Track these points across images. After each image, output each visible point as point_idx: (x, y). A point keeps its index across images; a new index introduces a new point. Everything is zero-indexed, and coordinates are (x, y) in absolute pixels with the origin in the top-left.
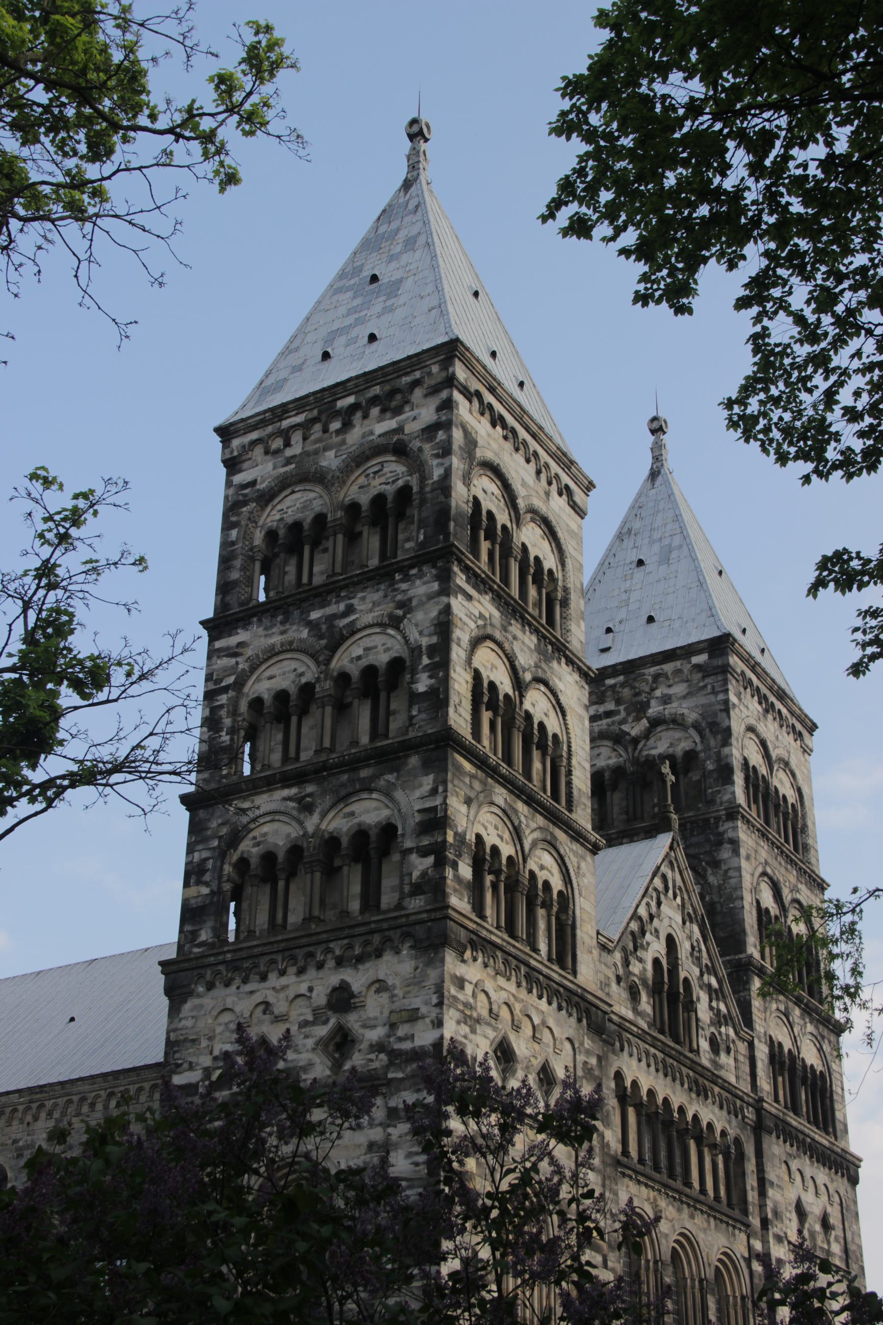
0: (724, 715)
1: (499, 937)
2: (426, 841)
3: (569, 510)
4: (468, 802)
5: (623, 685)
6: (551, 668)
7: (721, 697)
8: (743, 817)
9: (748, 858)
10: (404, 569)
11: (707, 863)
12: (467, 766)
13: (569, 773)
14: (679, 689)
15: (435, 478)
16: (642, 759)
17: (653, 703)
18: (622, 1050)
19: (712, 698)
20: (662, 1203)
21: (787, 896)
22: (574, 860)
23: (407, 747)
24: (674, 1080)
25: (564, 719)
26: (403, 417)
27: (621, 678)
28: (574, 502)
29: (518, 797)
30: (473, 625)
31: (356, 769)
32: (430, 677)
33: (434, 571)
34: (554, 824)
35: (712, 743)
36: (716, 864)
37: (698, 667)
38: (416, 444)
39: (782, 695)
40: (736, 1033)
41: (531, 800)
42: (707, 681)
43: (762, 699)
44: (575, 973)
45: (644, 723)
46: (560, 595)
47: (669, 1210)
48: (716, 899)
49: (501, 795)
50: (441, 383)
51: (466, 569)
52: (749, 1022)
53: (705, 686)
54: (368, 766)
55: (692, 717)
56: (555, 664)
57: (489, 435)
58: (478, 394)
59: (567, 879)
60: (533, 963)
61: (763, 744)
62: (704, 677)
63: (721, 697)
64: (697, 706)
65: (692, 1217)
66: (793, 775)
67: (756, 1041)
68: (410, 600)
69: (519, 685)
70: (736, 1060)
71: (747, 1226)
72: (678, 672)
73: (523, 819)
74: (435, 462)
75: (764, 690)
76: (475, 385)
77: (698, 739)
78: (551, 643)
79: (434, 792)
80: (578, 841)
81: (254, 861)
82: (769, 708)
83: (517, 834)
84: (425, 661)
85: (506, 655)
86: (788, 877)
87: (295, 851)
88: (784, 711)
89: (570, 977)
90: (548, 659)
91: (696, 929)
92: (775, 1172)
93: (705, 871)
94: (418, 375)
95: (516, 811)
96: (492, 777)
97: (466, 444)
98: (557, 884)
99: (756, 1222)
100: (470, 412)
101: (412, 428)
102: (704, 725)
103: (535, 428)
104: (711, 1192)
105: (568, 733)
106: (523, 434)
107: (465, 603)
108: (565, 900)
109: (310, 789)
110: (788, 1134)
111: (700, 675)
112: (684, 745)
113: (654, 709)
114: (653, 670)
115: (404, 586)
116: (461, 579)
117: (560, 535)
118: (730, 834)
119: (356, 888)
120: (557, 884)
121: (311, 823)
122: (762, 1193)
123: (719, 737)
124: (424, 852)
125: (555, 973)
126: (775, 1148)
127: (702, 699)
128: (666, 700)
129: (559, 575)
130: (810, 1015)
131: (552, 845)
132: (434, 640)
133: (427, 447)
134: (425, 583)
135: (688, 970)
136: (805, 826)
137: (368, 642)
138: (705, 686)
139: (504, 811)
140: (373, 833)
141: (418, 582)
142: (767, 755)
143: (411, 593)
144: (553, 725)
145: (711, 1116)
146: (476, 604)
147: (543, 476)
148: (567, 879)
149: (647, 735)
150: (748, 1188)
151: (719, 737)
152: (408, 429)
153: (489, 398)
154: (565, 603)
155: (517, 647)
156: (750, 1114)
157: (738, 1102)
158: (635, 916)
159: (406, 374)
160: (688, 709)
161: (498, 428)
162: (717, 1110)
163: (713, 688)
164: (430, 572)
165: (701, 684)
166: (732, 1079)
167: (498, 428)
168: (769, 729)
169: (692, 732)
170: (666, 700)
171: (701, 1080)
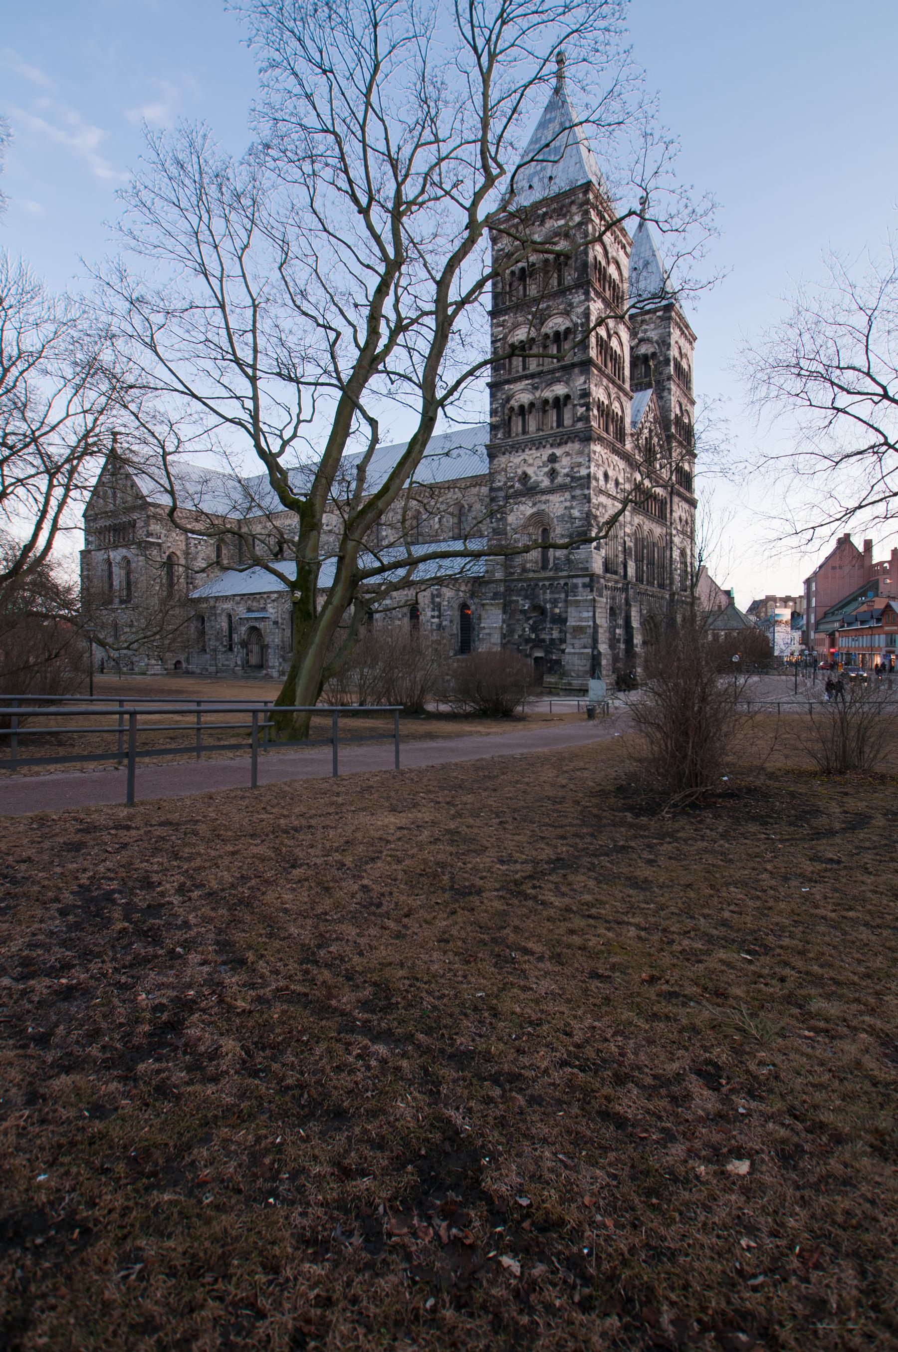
1: (605, 435)
2: (582, 401)
23: (573, 365)
37: (659, 317)
39: (687, 327)
41: (613, 382)
43: (681, 329)
47: (647, 522)
49: (605, 382)
55: (655, 338)
79: (585, 382)
81: (516, 408)
82: (683, 333)
83: (609, 396)
86: (684, 401)
87: (532, 405)
98: (620, 413)
109: (537, 380)
112: (652, 350)
113: (640, 335)
119: (555, 418)
120: (620, 413)
121: (537, 394)
124: (582, 406)
125: (619, 445)
127: (660, 331)
128: (645, 331)
131: (619, 398)
142: (680, 353)
144: (619, 352)
148: (623, 411)
160: (654, 335)
168: (682, 341)
170: (645, 331)
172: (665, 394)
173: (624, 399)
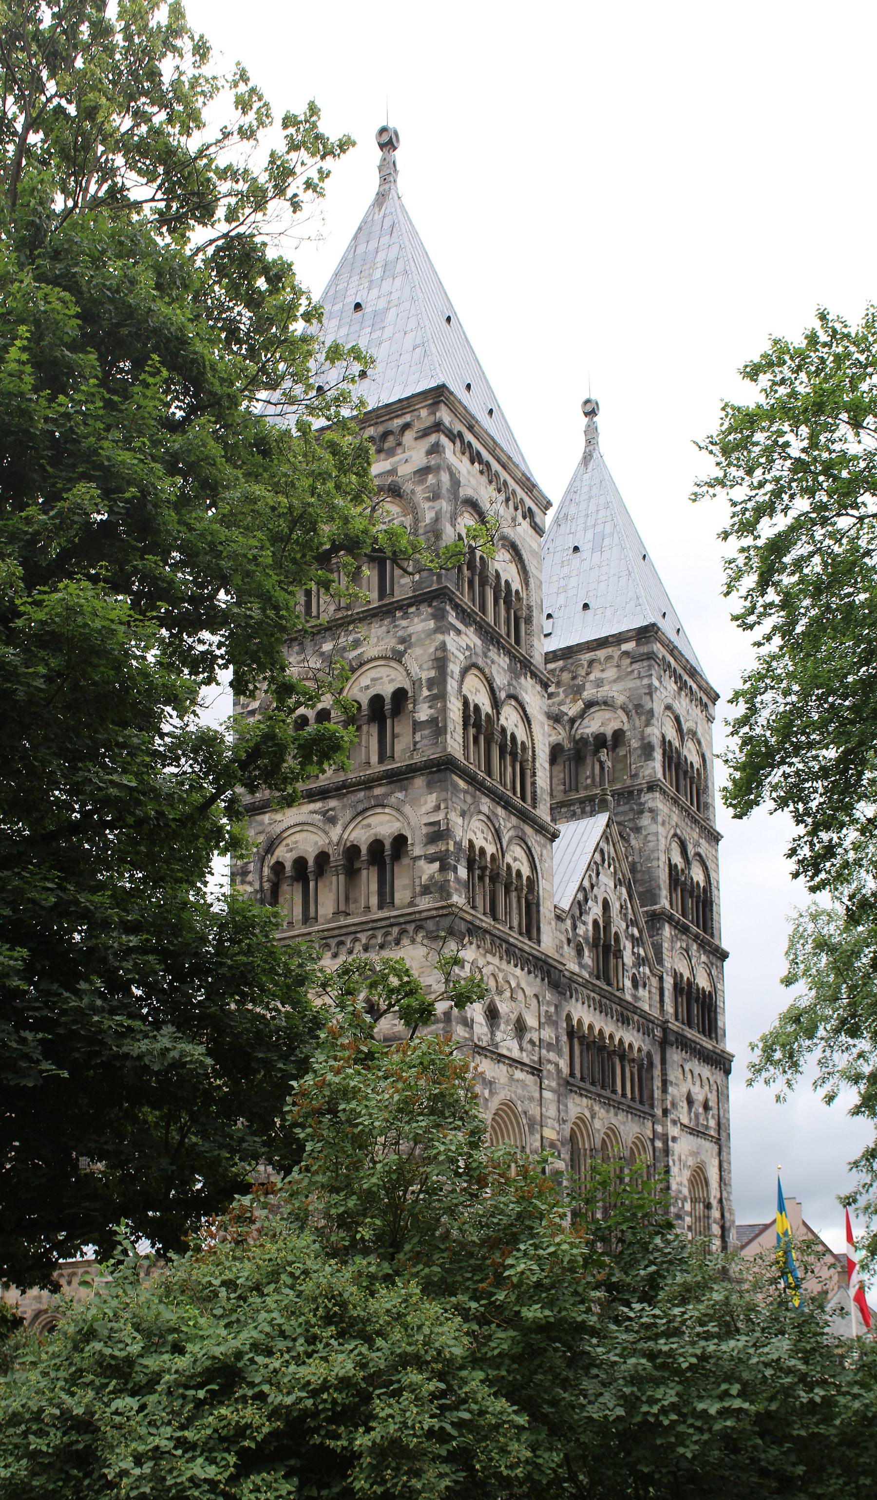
0: (648, 697)
1: (487, 922)
2: (432, 850)
3: (531, 531)
4: (463, 814)
5: (562, 670)
6: (520, 684)
7: (645, 681)
8: (661, 789)
9: (663, 824)
10: (403, 607)
11: (631, 829)
12: (462, 784)
13: (534, 774)
14: (611, 673)
15: (428, 521)
16: (578, 737)
17: (587, 685)
18: (571, 997)
19: (638, 682)
20: (596, 1108)
21: (691, 851)
22: (538, 849)
23: (412, 770)
24: (606, 1015)
25: (530, 728)
26: (396, 459)
27: (560, 663)
28: (535, 523)
29: (498, 803)
30: (462, 657)
31: (370, 788)
32: (430, 707)
33: (430, 610)
34: (524, 821)
35: (637, 723)
36: (637, 830)
37: (626, 654)
38: (408, 487)
39: (693, 673)
40: (651, 971)
41: (507, 805)
42: (635, 666)
43: (678, 679)
44: (539, 942)
45: (580, 705)
46: (524, 613)
47: (601, 1112)
48: (637, 860)
49: (486, 804)
50: (430, 427)
51: (456, 607)
52: (660, 961)
53: (632, 671)
54: (380, 785)
55: (620, 699)
56: (522, 680)
57: (469, 473)
58: (460, 435)
59: (533, 867)
60: (512, 940)
61: (677, 719)
62: (632, 663)
63: (645, 681)
64: (625, 690)
65: (616, 1115)
66: (699, 743)
67: (665, 975)
68: (410, 636)
69: (496, 704)
70: (650, 992)
71: (653, 1116)
72: (609, 658)
73: (502, 822)
74: (427, 505)
75: (680, 670)
76: (458, 427)
77: (625, 719)
78: (520, 662)
79: (437, 808)
80: (540, 833)
81: (288, 866)
82: (683, 686)
83: (498, 835)
84: (425, 693)
85: (487, 679)
86: (691, 834)
87: (323, 858)
88: (694, 686)
89: (537, 947)
90: (517, 677)
91: (624, 890)
92: (674, 1075)
93: (629, 835)
94: (408, 418)
95: (497, 816)
96: (479, 790)
97: (452, 486)
98: (526, 871)
99: (659, 1112)
100: (454, 453)
101: (405, 470)
102: (630, 707)
103: (504, 459)
104: (629, 1095)
105: (532, 740)
106: (495, 466)
107: (456, 638)
108: (532, 883)
109: (333, 803)
110: (684, 1044)
111: (628, 661)
112: (615, 725)
113: (589, 693)
114: (589, 656)
115: (404, 623)
116: (452, 617)
117: (525, 557)
118: (650, 804)
119: (374, 887)
120: (526, 871)
121: (335, 833)
122: (664, 1091)
123: (643, 718)
124: (431, 860)
125: (526, 944)
126: (675, 1056)
127: (631, 684)
128: (599, 683)
129: (523, 595)
130: (703, 947)
131: (522, 839)
132: (433, 674)
133: (419, 489)
134: (422, 621)
135: (618, 925)
136: (707, 787)
137: (373, 674)
138: (632, 671)
139: (488, 817)
140: (388, 843)
141: (416, 620)
142: (679, 729)
143: (411, 630)
144: (521, 736)
145: (632, 1039)
146: (463, 636)
147: (511, 503)
148: (533, 867)
149: (582, 715)
150: (655, 1088)
151: (643, 718)
152: (401, 471)
153: (469, 437)
154: (529, 620)
155: (494, 670)
156: (658, 1033)
157: (651, 1025)
158: (581, 888)
159: (397, 417)
160: (617, 692)
161: (476, 464)
162: (635, 1033)
163: (639, 673)
164: (426, 610)
165: (629, 670)
166: (646, 1008)
167: (476, 464)
168: (682, 705)
169: (620, 712)
170: (599, 683)
171: (625, 1012)
172: (645, 821)
173: (534, 839)
